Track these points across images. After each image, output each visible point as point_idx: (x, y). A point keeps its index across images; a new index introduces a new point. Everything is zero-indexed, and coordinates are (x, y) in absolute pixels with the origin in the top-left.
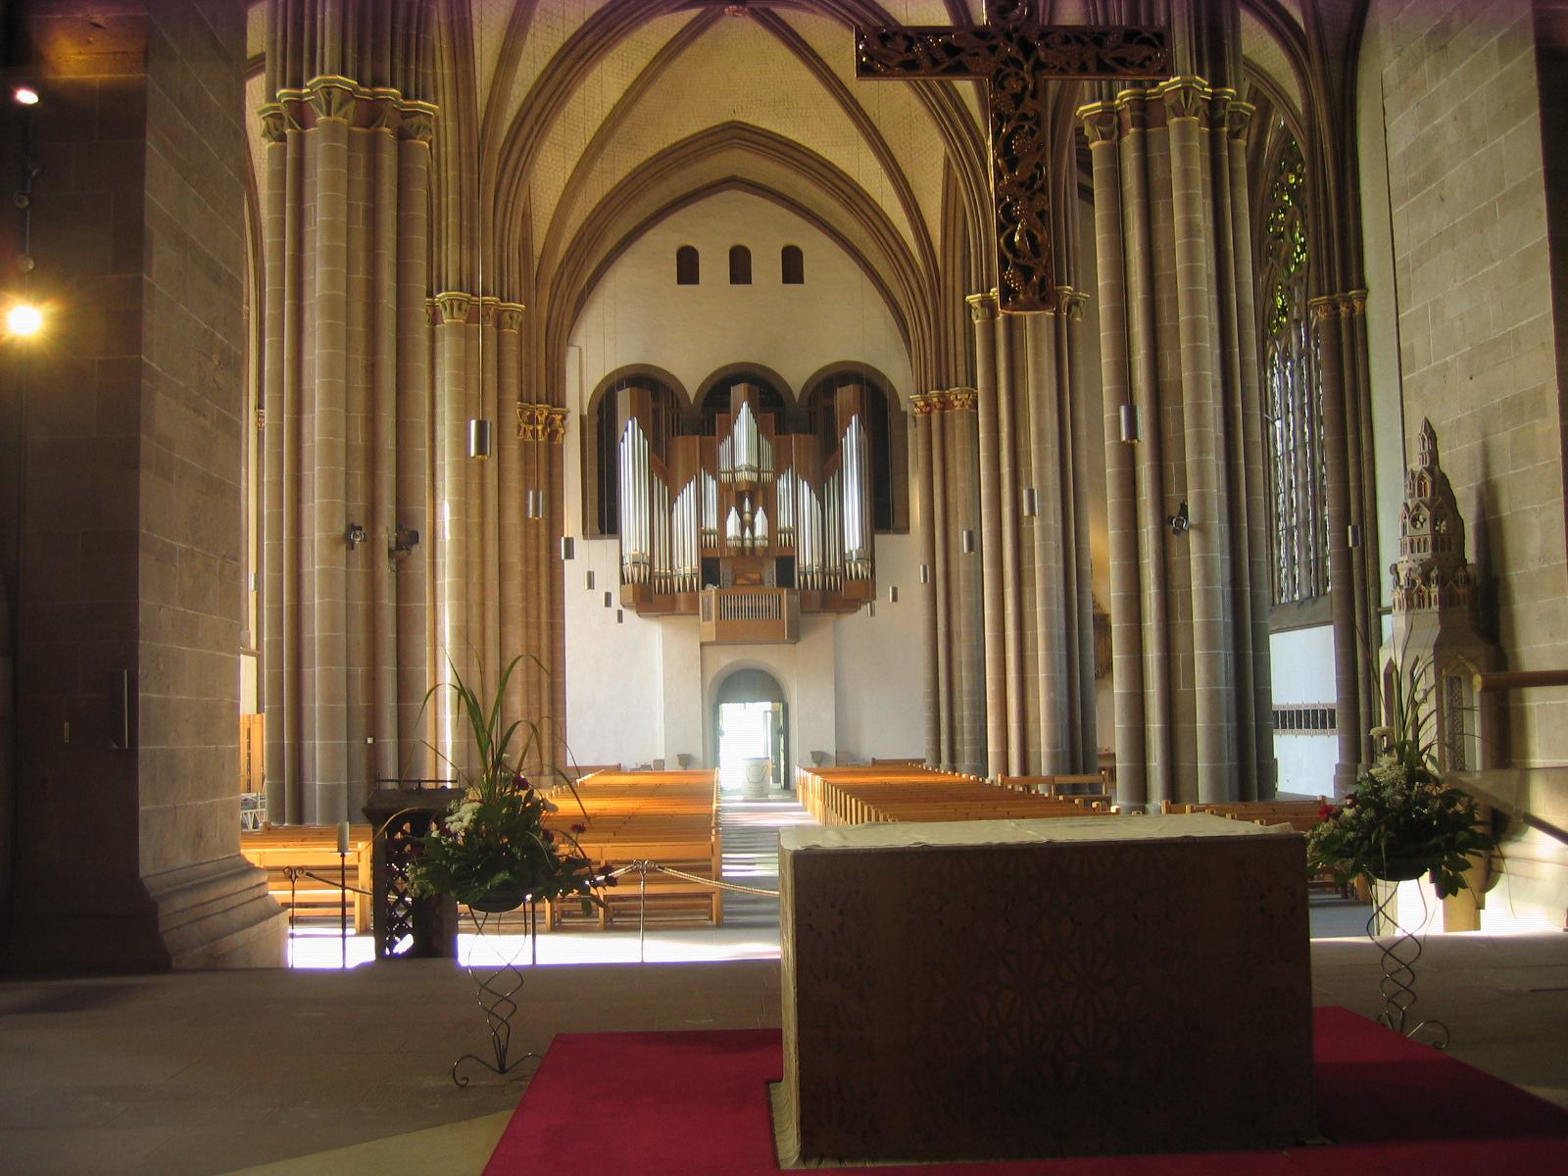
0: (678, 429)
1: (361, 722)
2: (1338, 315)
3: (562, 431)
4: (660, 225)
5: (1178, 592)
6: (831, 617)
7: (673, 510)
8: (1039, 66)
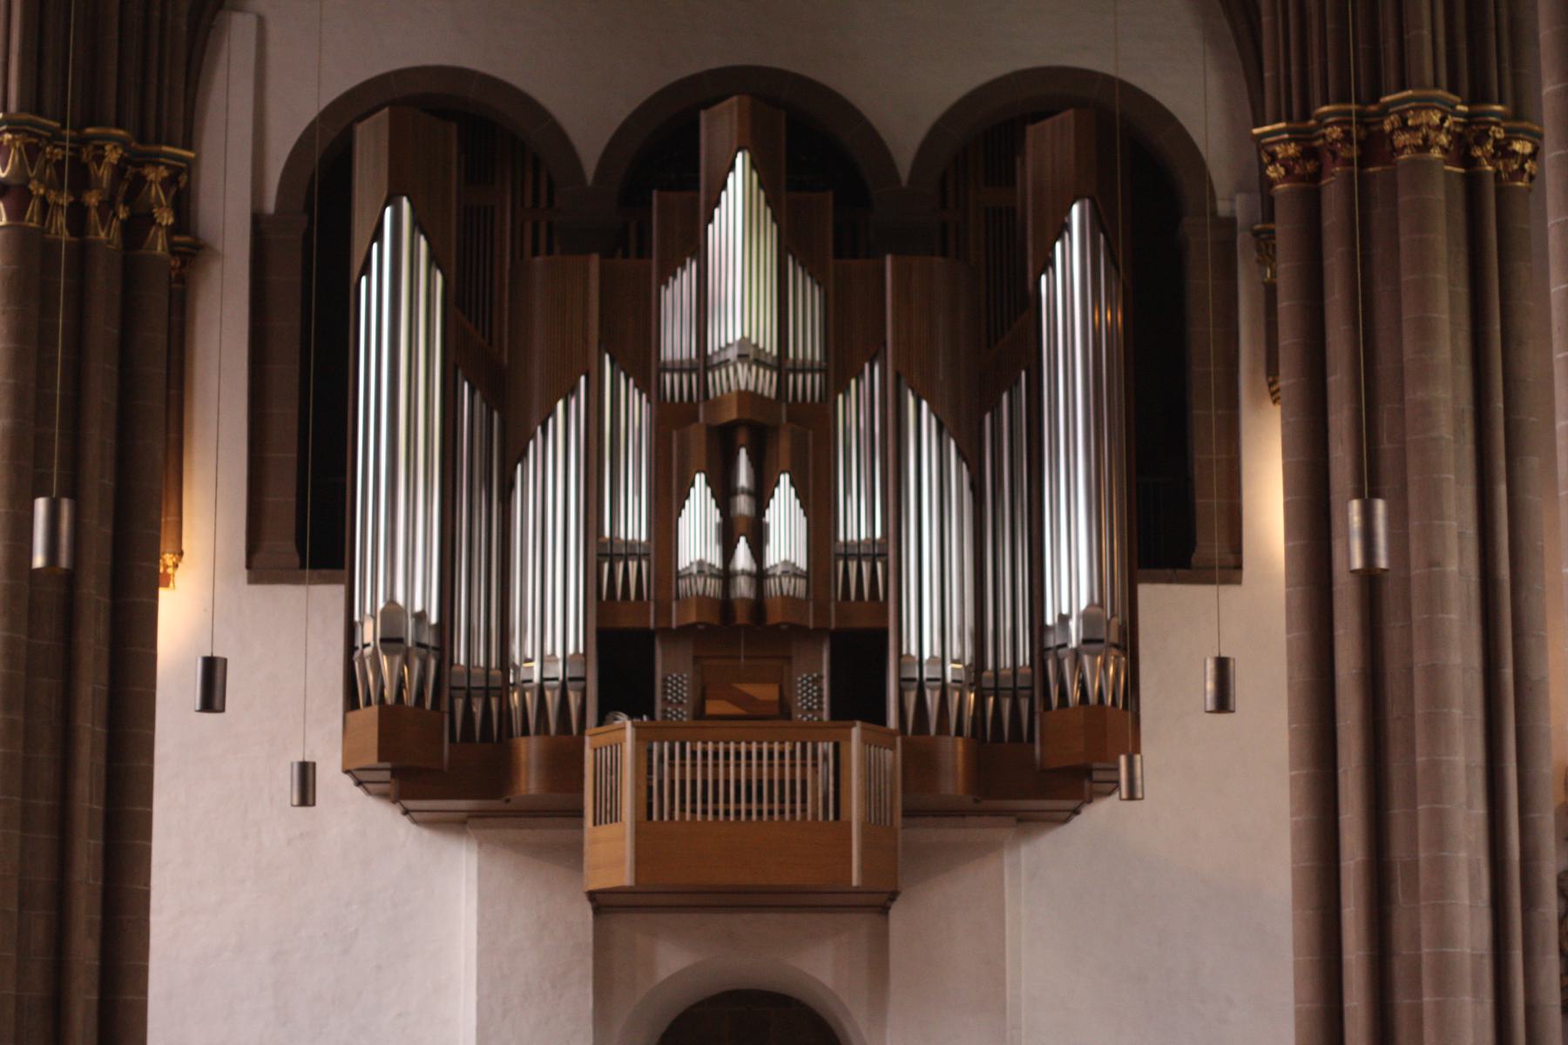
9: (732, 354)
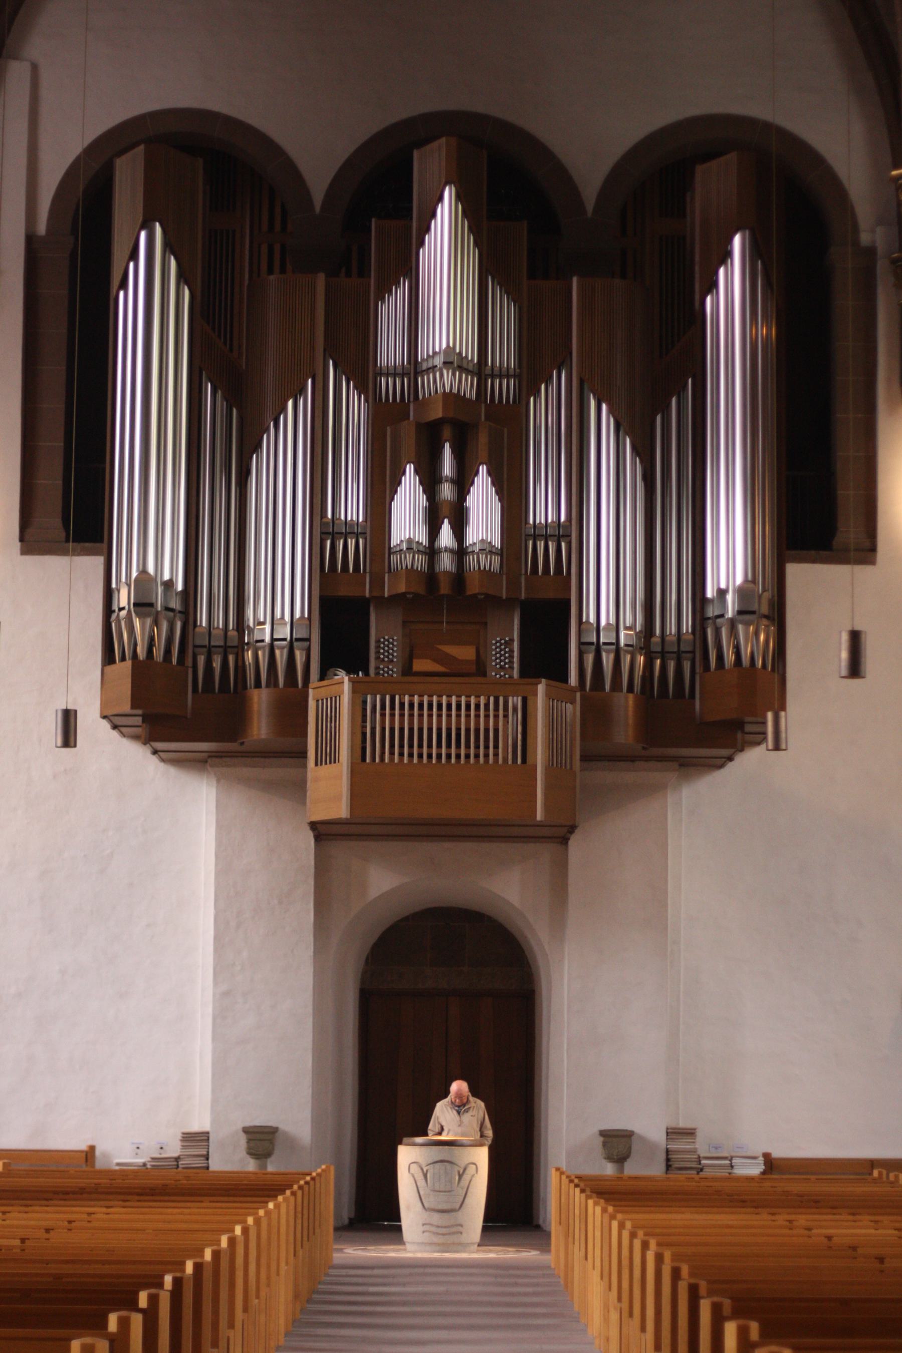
7: (249, 472)
9: (438, 361)
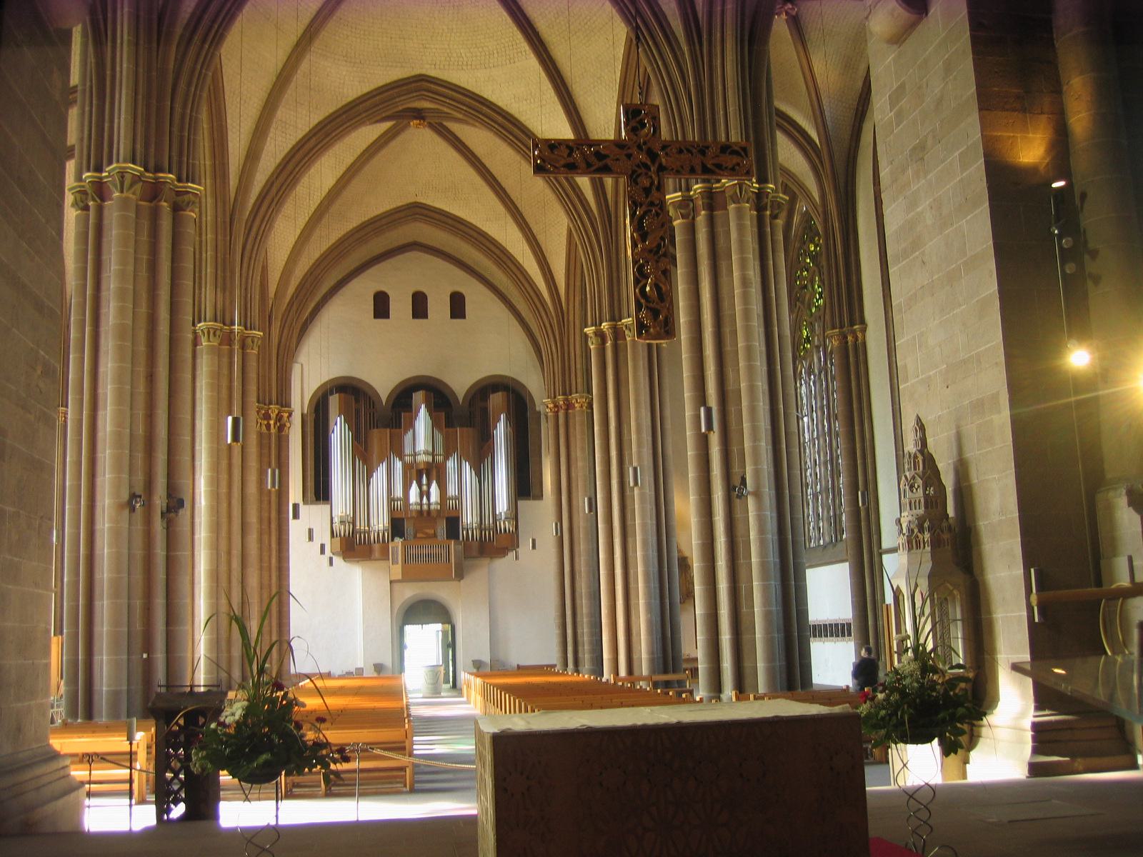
0: (375, 423)
1: (138, 643)
2: (847, 342)
3: (288, 425)
4: (362, 275)
5: (740, 540)
6: (486, 561)
8: (661, 168)
